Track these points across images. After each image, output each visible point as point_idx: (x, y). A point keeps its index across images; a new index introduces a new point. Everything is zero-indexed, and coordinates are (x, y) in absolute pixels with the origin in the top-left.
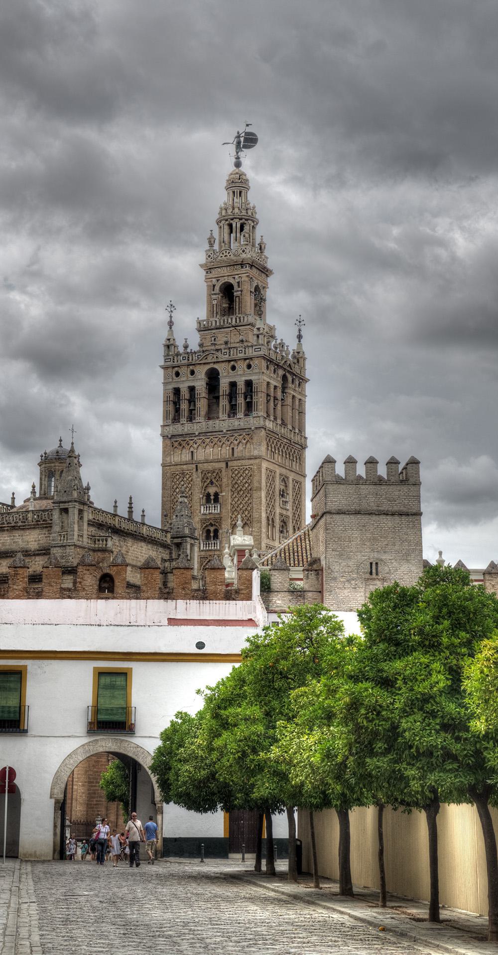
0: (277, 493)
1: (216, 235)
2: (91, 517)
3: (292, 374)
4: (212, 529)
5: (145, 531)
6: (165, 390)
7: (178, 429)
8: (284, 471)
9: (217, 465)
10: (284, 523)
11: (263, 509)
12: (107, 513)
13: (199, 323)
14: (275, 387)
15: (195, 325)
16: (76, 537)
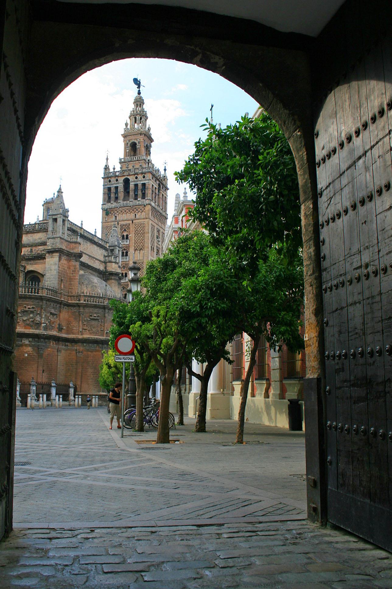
0: (155, 236)
1: (129, 122)
2: (69, 226)
3: (163, 184)
4: (125, 252)
5: (96, 240)
6: (104, 188)
7: (108, 206)
8: (158, 227)
9: (128, 222)
10: (157, 250)
11: (150, 242)
12: (78, 226)
13: (120, 159)
14: (156, 188)
15: (119, 161)
16: (61, 233)
